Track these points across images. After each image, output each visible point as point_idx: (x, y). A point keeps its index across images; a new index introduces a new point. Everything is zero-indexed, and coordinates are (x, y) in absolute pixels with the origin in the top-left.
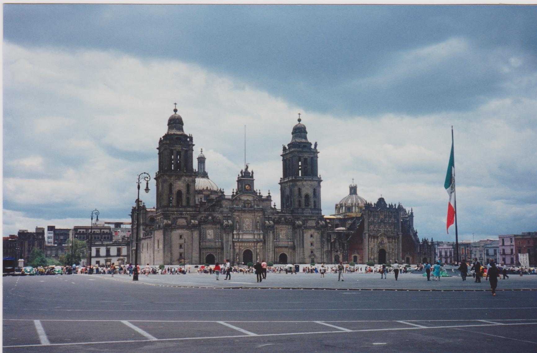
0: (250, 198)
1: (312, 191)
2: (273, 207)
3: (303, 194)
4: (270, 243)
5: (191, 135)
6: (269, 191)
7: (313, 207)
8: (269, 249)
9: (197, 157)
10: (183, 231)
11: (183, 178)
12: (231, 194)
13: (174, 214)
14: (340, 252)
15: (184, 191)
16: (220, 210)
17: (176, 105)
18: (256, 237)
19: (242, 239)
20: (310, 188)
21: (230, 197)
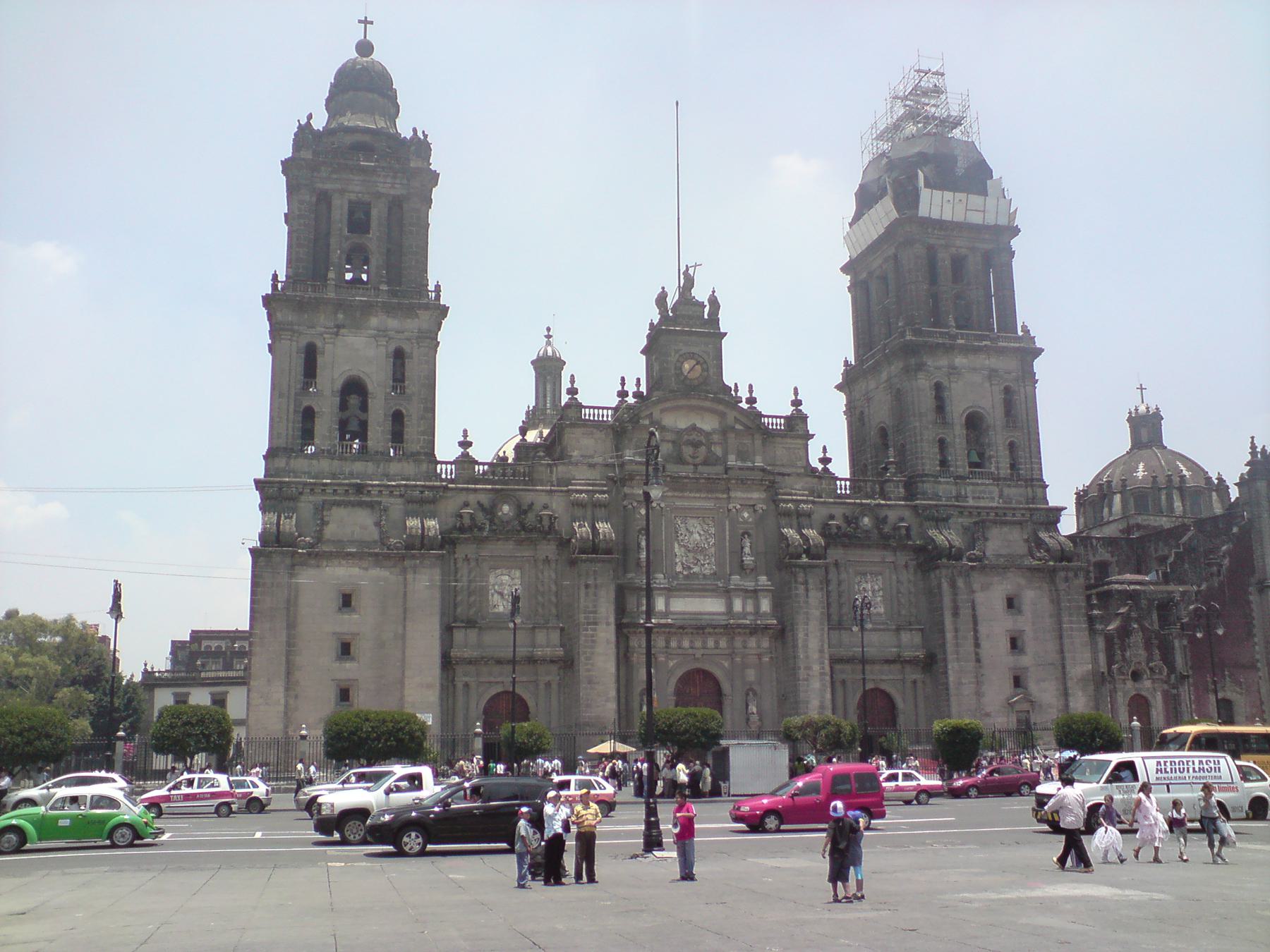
0: (708, 424)
1: (999, 397)
2: (815, 463)
3: (958, 409)
4: (807, 635)
5: (420, 135)
6: (796, 392)
7: (1005, 471)
8: (808, 668)
9: (535, 358)
10: (357, 569)
11: (374, 321)
12: (614, 401)
13: (318, 490)
14: (1154, 681)
15: (377, 377)
16: (554, 476)
17: (368, 25)
18: (738, 605)
19: (666, 614)
20: (987, 384)
21: (608, 416)
